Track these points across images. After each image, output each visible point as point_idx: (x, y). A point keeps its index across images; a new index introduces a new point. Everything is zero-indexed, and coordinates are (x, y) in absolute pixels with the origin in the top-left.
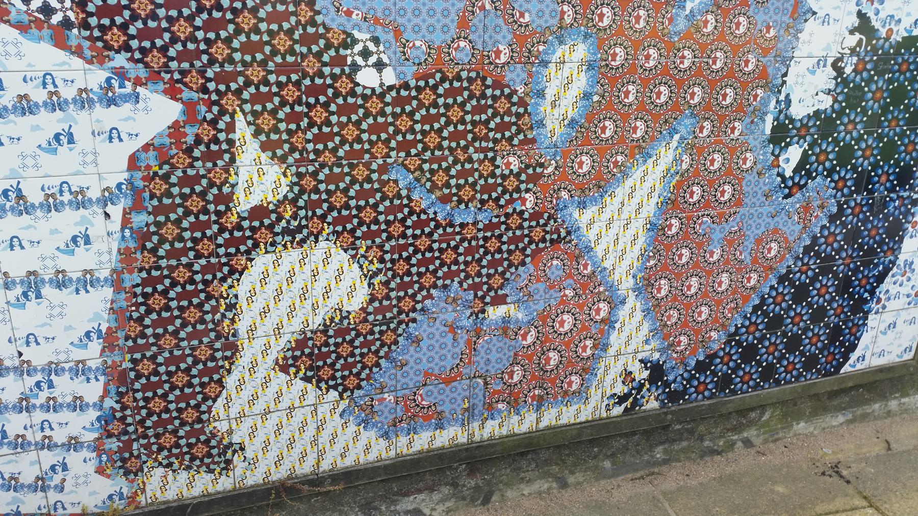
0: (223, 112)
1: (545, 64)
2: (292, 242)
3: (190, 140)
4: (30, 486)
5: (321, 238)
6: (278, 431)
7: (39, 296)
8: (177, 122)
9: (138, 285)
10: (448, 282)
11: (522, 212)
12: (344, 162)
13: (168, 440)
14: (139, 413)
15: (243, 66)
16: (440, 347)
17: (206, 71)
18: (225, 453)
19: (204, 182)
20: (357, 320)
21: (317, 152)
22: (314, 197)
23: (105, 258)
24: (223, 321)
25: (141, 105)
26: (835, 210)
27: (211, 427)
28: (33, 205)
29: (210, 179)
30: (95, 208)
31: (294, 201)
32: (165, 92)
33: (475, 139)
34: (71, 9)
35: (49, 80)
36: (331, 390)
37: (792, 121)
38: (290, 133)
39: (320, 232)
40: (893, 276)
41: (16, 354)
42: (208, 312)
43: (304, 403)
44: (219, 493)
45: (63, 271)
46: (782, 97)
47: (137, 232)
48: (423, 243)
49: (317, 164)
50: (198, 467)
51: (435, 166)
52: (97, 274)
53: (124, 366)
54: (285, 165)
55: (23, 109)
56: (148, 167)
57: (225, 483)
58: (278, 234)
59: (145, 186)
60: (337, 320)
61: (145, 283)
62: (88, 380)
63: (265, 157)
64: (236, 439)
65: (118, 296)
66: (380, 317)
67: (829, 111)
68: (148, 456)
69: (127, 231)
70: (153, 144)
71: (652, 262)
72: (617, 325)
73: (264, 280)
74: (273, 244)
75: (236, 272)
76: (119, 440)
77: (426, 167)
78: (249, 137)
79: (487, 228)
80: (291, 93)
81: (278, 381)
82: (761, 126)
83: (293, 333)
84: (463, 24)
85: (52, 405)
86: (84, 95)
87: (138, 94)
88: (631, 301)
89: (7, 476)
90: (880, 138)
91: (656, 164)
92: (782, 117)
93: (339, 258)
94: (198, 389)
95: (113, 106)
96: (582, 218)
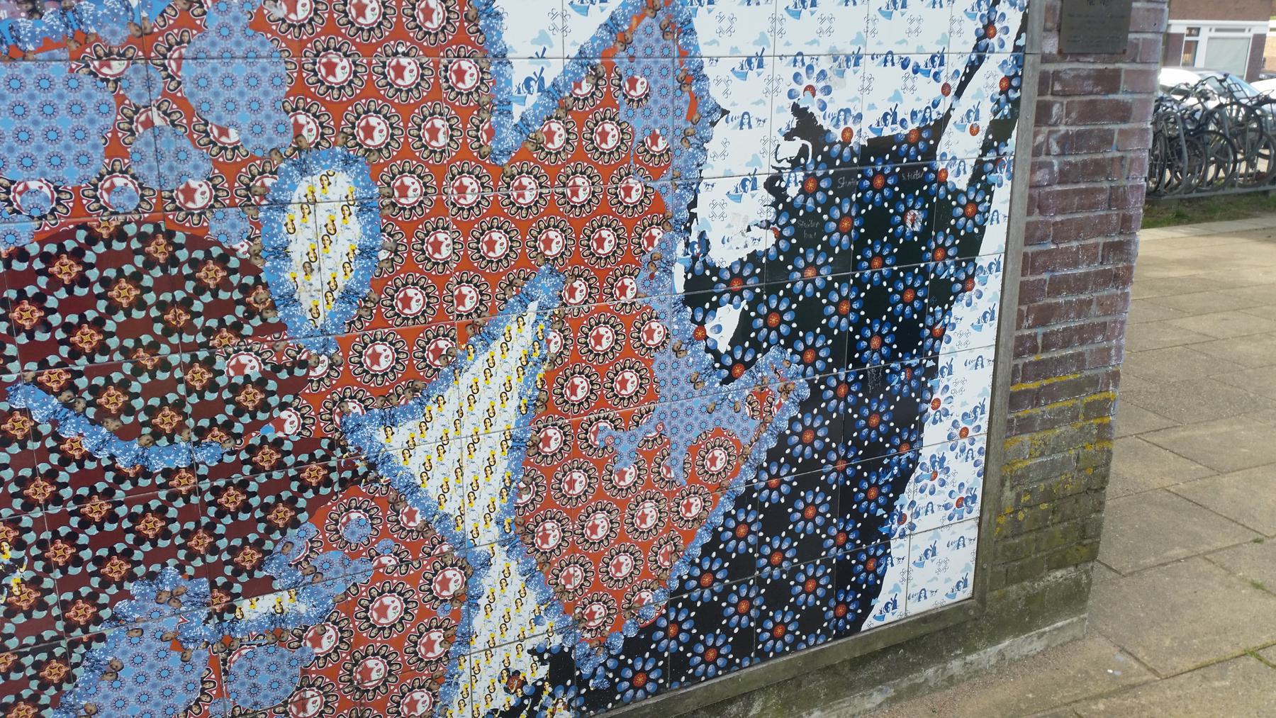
1: (282, 206)
10: (156, 568)
11: (278, 443)
16: (159, 675)
26: (807, 393)
33: (168, 331)
37: (716, 270)
40: (917, 481)
46: (694, 237)
48: (96, 509)
51: (99, 381)
66: (31, 640)
67: (772, 252)
71: (526, 498)
72: (483, 602)
77: (82, 383)
79: (214, 473)
82: (667, 282)
84: (115, 149)
88: (500, 560)
90: (859, 285)
91: (505, 348)
92: (698, 266)
96: (394, 440)
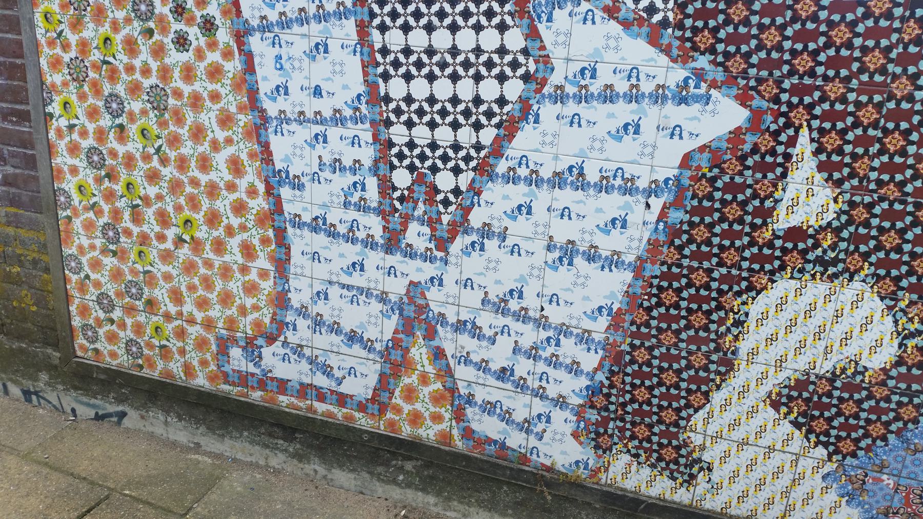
0: (788, 125)
2: (822, 274)
3: (747, 148)
4: (518, 424)
5: (856, 278)
6: (751, 467)
7: (570, 264)
8: (739, 128)
9: (656, 277)
12: (910, 199)
13: (642, 431)
14: (623, 396)
15: (824, 80)
17: (783, 82)
18: (692, 467)
19: (749, 192)
20: (874, 381)
21: (880, 183)
22: (862, 231)
23: (635, 244)
24: (726, 335)
25: (710, 107)
27: (685, 436)
28: (589, 183)
29: (755, 190)
30: (639, 197)
31: (837, 231)
32: (737, 97)
34: (672, 10)
35: (634, 74)
36: (820, 447)
38: (855, 156)
39: (857, 271)
41: (539, 308)
42: (714, 322)
43: (786, 449)
44: (675, 503)
45: (596, 247)
47: (669, 227)
49: (875, 196)
50: (663, 469)
52: (623, 257)
53: (622, 348)
54: (839, 190)
55: (606, 97)
56: (699, 168)
57: (683, 496)
58: (809, 261)
59: (690, 185)
60: (849, 372)
61: (662, 277)
62: (589, 350)
63: (819, 178)
64: (706, 457)
65: (636, 282)
66: (903, 386)
68: (620, 439)
69: (661, 224)
70: (710, 147)
73: (781, 305)
74: (802, 271)
75: (754, 290)
76: (599, 414)
78: (808, 154)
80: (868, 115)
81: (766, 415)
83: (796, 371)
85: (554, 362)
86: (660, 91)
87: (710, 96)
89: (504, 408)
93: (872, 305)
94: (683, 394)
95: (683, 105)
